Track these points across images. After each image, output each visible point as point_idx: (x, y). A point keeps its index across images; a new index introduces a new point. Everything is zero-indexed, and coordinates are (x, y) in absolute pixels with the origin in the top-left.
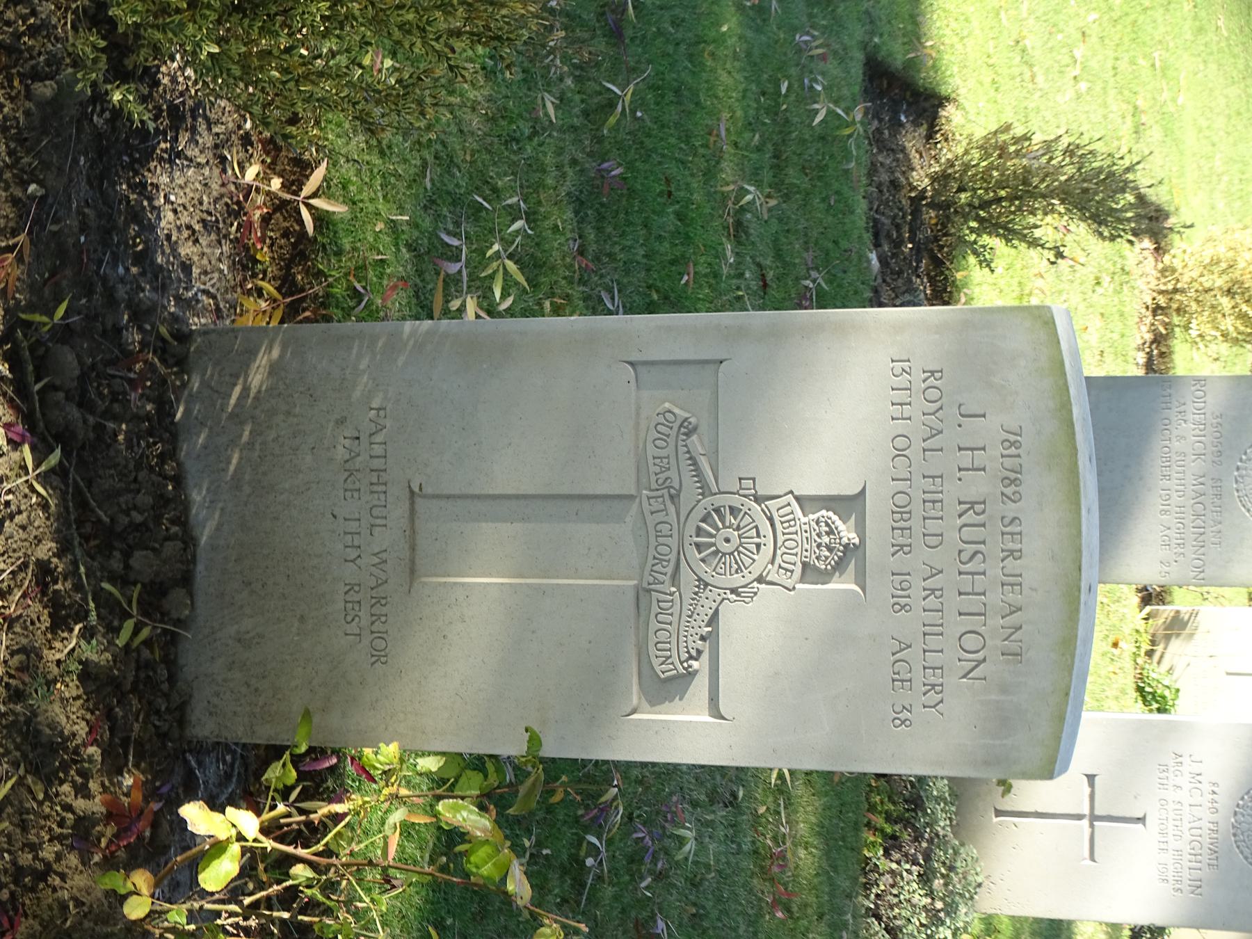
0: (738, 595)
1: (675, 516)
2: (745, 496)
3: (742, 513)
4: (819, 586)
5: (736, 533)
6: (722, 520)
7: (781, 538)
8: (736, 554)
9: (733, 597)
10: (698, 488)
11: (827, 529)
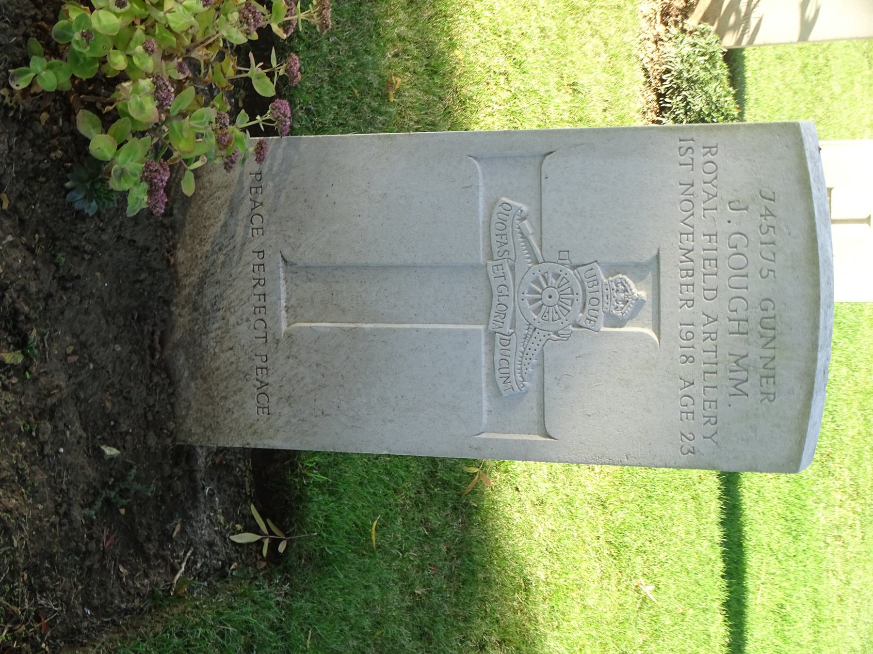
0: (559, 336)
1: (511, 280)
2: (562, 264)
3: (561, 278)
4: (617, 330)
5: (556, 291)
7: (589, 296)
8: (556, 306)
9: (556, 337)
10: (528, 258)
11: (623, 287)
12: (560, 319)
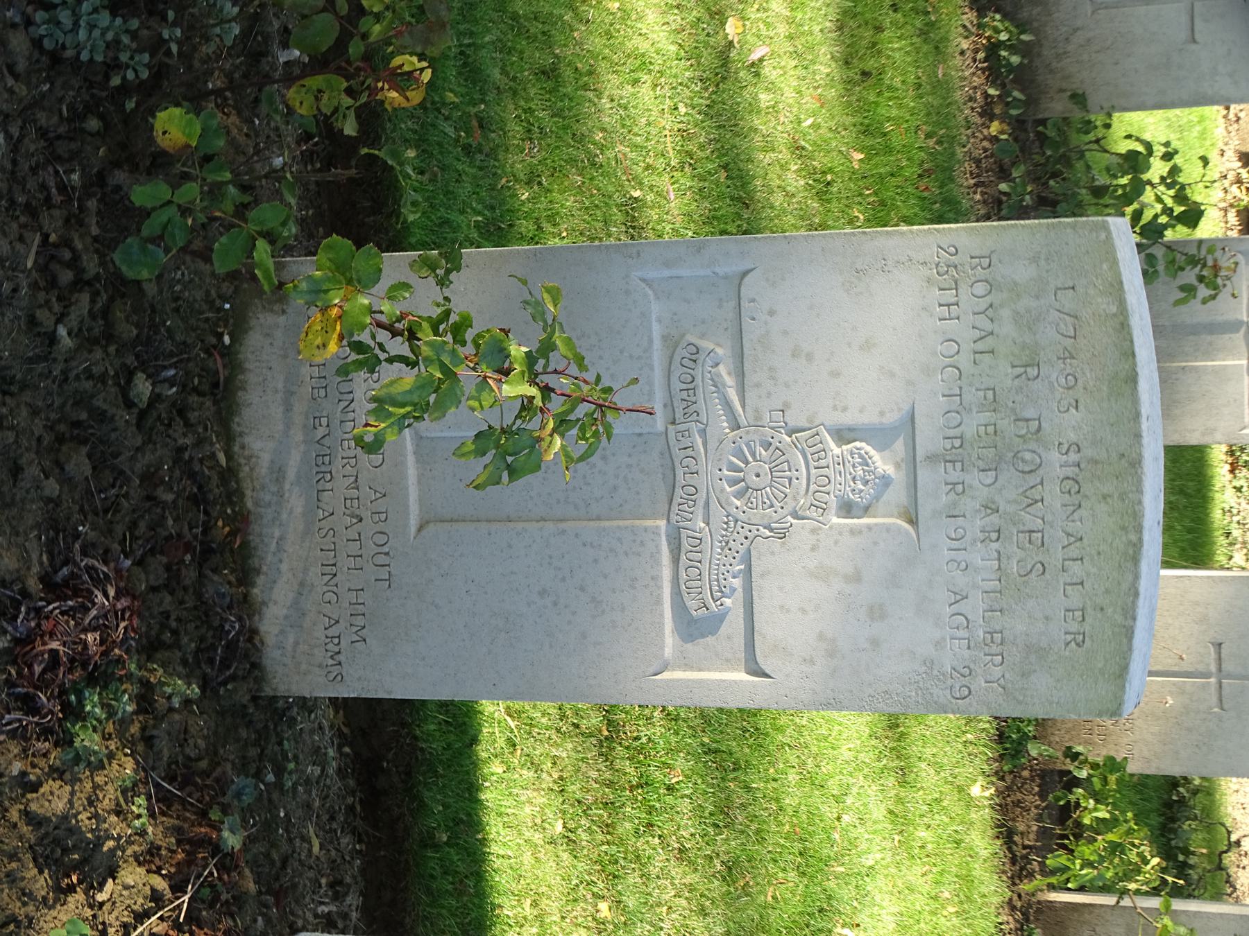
0: (771, 530)
3: (772, 448)
5: (767, 466)
6: (753, 455)
7: (813, 471)
8: (768, 489)
9: (768, 533)
12: (772, 506)
